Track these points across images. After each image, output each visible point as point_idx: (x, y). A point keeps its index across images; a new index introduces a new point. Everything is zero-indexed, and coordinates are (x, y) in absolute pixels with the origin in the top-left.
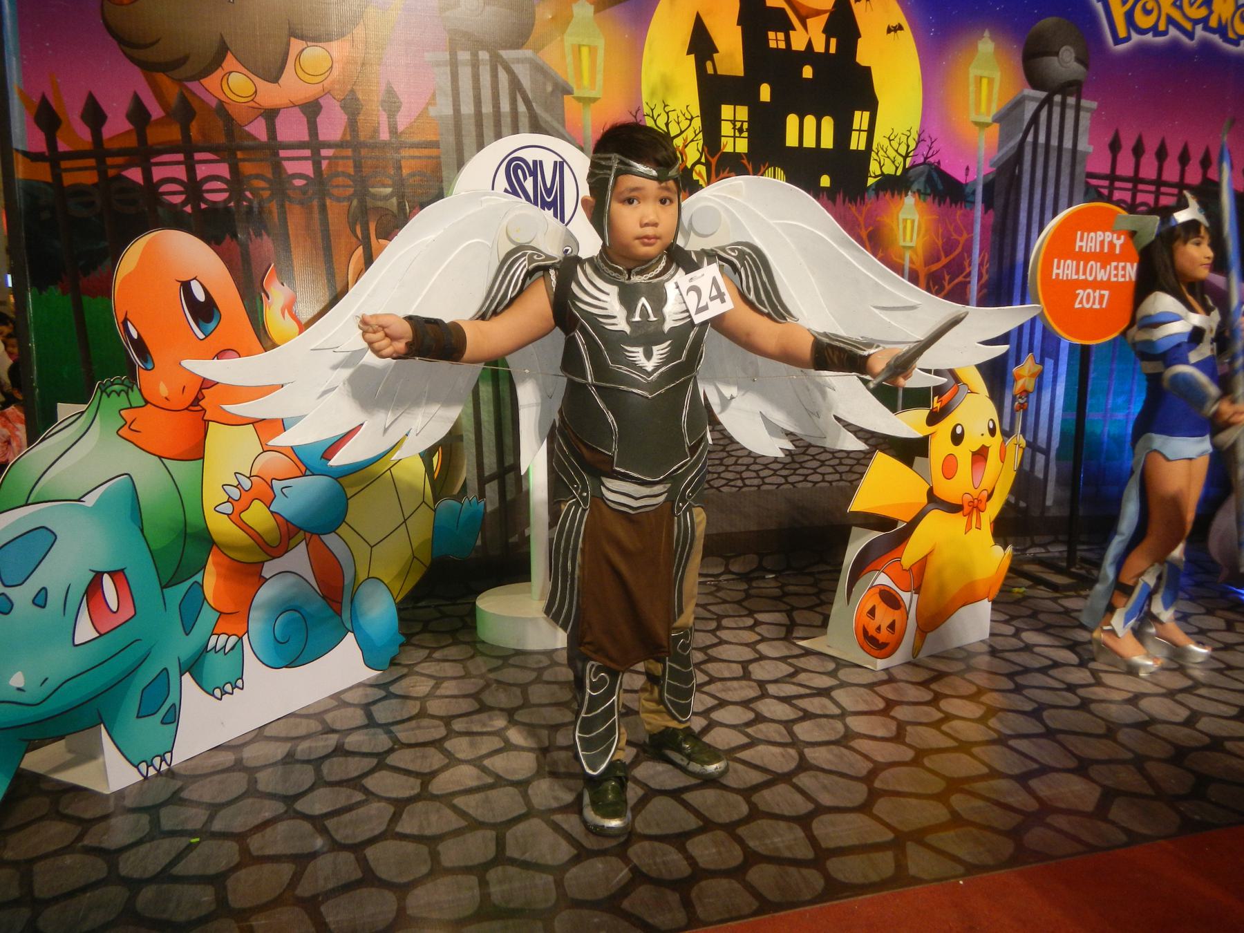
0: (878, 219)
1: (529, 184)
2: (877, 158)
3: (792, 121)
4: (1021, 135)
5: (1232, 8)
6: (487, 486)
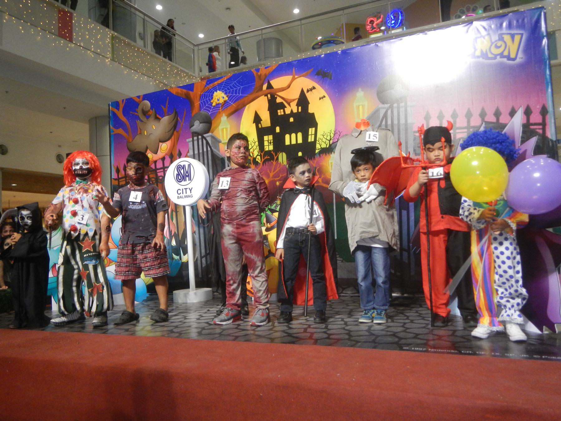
0: (321, 164)
1: (182, 171)
2: (319, 143)
3: (287, 136)
4: (379, 123)
5: (490, 44)
6: (203, 259)
